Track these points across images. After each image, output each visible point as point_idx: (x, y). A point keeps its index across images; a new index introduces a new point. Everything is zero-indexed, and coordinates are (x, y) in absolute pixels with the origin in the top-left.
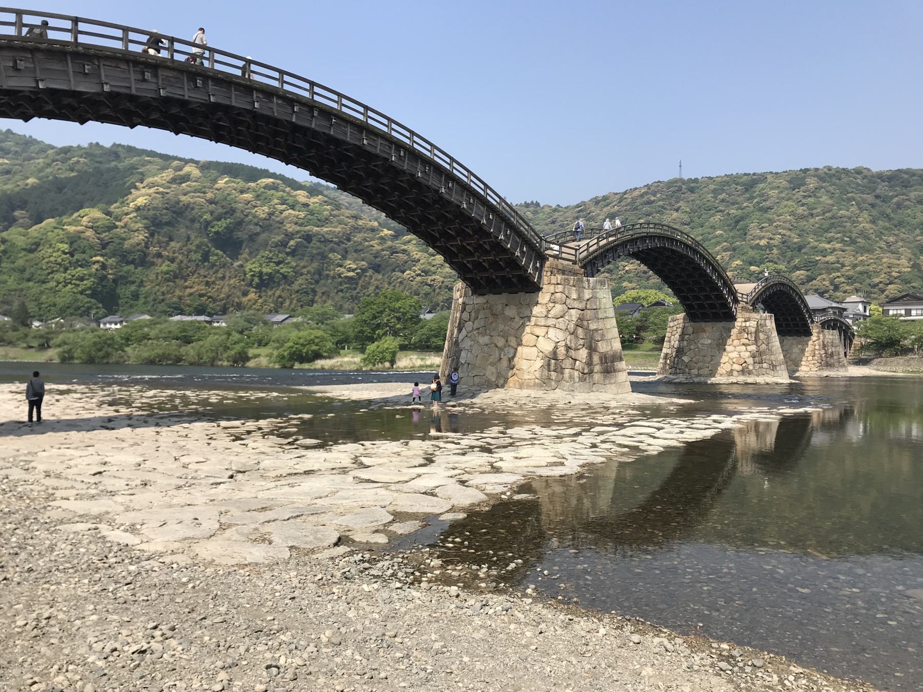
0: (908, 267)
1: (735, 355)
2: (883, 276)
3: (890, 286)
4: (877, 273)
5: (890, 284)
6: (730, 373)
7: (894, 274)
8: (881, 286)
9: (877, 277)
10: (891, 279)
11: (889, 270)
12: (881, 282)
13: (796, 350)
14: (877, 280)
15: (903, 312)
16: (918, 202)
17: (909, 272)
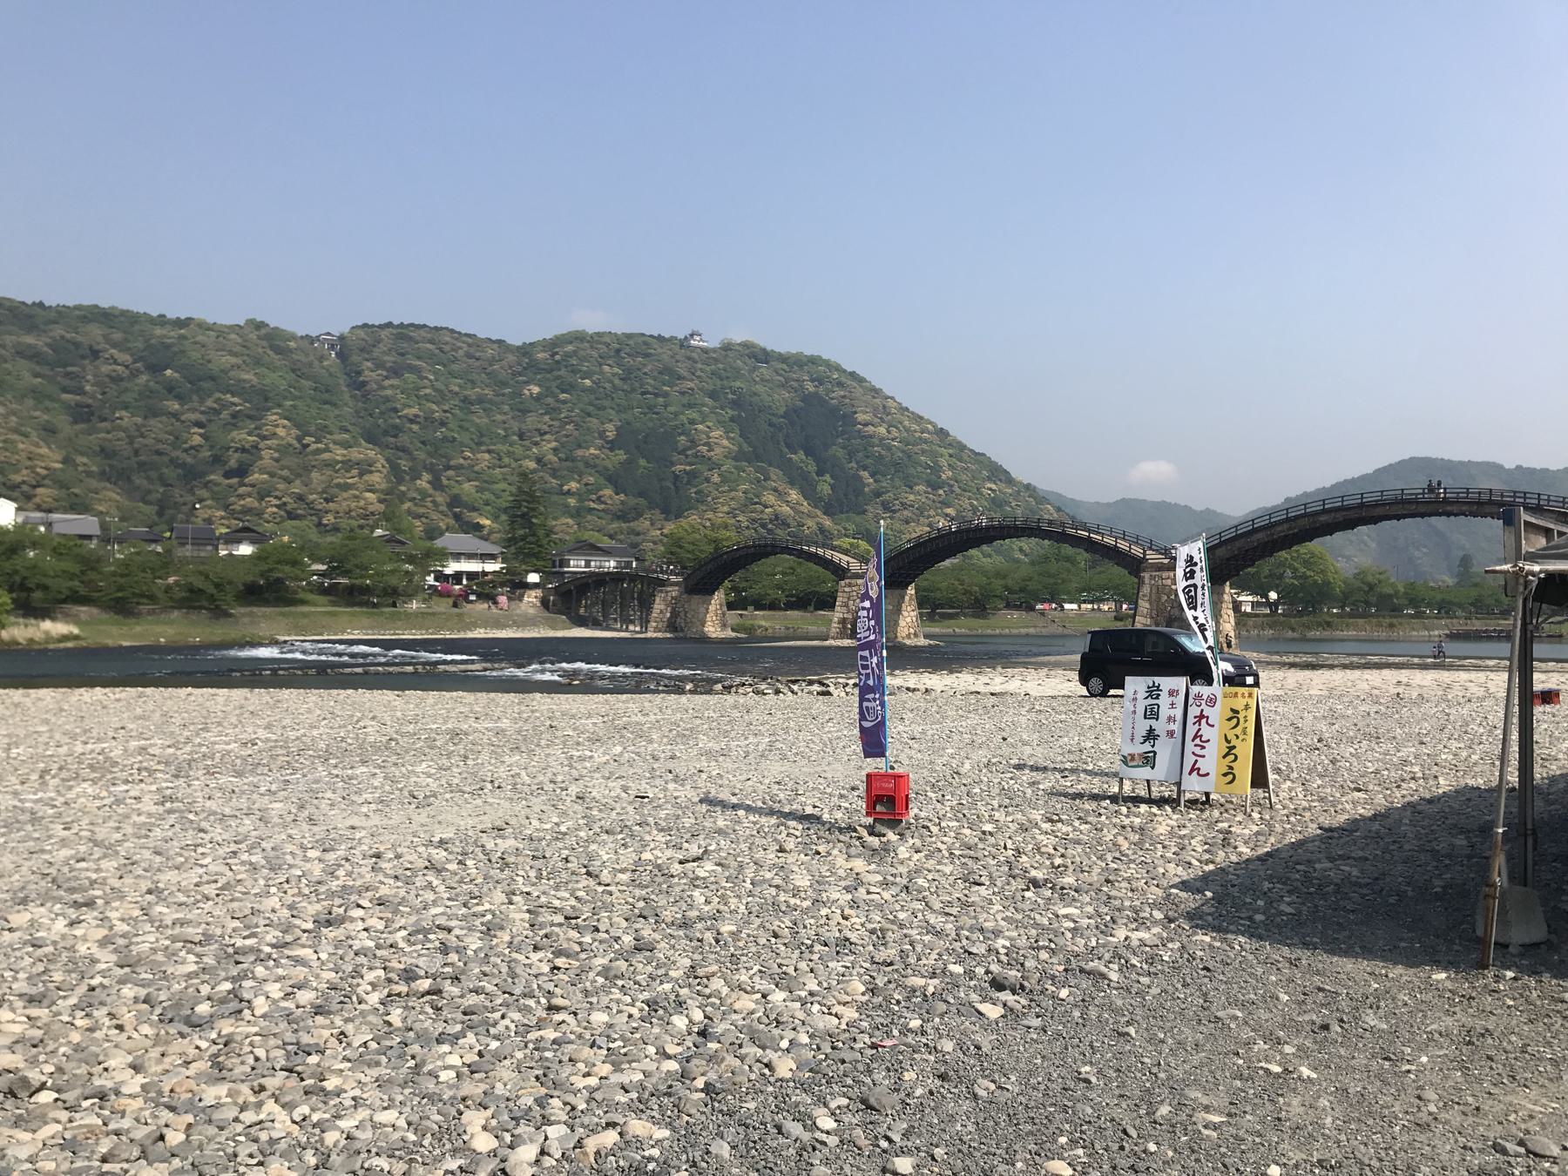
0: (58, 462)
1: (909, 620)
2: (25, 472)
3: (40, 490)
4: (16, 468)
5: (39, 486)
6: (909, 636)
7: (38, 470)
8: (25, 488)
9: (17, 471)
10: (38, 478)
11: (29, 463)
12: (24, 482)
13: (702, 610)
14: (17, 478)
15: (583, 563)
16: (18, 353)
17: (62, 470)
